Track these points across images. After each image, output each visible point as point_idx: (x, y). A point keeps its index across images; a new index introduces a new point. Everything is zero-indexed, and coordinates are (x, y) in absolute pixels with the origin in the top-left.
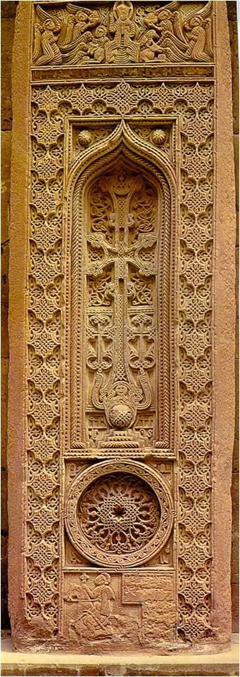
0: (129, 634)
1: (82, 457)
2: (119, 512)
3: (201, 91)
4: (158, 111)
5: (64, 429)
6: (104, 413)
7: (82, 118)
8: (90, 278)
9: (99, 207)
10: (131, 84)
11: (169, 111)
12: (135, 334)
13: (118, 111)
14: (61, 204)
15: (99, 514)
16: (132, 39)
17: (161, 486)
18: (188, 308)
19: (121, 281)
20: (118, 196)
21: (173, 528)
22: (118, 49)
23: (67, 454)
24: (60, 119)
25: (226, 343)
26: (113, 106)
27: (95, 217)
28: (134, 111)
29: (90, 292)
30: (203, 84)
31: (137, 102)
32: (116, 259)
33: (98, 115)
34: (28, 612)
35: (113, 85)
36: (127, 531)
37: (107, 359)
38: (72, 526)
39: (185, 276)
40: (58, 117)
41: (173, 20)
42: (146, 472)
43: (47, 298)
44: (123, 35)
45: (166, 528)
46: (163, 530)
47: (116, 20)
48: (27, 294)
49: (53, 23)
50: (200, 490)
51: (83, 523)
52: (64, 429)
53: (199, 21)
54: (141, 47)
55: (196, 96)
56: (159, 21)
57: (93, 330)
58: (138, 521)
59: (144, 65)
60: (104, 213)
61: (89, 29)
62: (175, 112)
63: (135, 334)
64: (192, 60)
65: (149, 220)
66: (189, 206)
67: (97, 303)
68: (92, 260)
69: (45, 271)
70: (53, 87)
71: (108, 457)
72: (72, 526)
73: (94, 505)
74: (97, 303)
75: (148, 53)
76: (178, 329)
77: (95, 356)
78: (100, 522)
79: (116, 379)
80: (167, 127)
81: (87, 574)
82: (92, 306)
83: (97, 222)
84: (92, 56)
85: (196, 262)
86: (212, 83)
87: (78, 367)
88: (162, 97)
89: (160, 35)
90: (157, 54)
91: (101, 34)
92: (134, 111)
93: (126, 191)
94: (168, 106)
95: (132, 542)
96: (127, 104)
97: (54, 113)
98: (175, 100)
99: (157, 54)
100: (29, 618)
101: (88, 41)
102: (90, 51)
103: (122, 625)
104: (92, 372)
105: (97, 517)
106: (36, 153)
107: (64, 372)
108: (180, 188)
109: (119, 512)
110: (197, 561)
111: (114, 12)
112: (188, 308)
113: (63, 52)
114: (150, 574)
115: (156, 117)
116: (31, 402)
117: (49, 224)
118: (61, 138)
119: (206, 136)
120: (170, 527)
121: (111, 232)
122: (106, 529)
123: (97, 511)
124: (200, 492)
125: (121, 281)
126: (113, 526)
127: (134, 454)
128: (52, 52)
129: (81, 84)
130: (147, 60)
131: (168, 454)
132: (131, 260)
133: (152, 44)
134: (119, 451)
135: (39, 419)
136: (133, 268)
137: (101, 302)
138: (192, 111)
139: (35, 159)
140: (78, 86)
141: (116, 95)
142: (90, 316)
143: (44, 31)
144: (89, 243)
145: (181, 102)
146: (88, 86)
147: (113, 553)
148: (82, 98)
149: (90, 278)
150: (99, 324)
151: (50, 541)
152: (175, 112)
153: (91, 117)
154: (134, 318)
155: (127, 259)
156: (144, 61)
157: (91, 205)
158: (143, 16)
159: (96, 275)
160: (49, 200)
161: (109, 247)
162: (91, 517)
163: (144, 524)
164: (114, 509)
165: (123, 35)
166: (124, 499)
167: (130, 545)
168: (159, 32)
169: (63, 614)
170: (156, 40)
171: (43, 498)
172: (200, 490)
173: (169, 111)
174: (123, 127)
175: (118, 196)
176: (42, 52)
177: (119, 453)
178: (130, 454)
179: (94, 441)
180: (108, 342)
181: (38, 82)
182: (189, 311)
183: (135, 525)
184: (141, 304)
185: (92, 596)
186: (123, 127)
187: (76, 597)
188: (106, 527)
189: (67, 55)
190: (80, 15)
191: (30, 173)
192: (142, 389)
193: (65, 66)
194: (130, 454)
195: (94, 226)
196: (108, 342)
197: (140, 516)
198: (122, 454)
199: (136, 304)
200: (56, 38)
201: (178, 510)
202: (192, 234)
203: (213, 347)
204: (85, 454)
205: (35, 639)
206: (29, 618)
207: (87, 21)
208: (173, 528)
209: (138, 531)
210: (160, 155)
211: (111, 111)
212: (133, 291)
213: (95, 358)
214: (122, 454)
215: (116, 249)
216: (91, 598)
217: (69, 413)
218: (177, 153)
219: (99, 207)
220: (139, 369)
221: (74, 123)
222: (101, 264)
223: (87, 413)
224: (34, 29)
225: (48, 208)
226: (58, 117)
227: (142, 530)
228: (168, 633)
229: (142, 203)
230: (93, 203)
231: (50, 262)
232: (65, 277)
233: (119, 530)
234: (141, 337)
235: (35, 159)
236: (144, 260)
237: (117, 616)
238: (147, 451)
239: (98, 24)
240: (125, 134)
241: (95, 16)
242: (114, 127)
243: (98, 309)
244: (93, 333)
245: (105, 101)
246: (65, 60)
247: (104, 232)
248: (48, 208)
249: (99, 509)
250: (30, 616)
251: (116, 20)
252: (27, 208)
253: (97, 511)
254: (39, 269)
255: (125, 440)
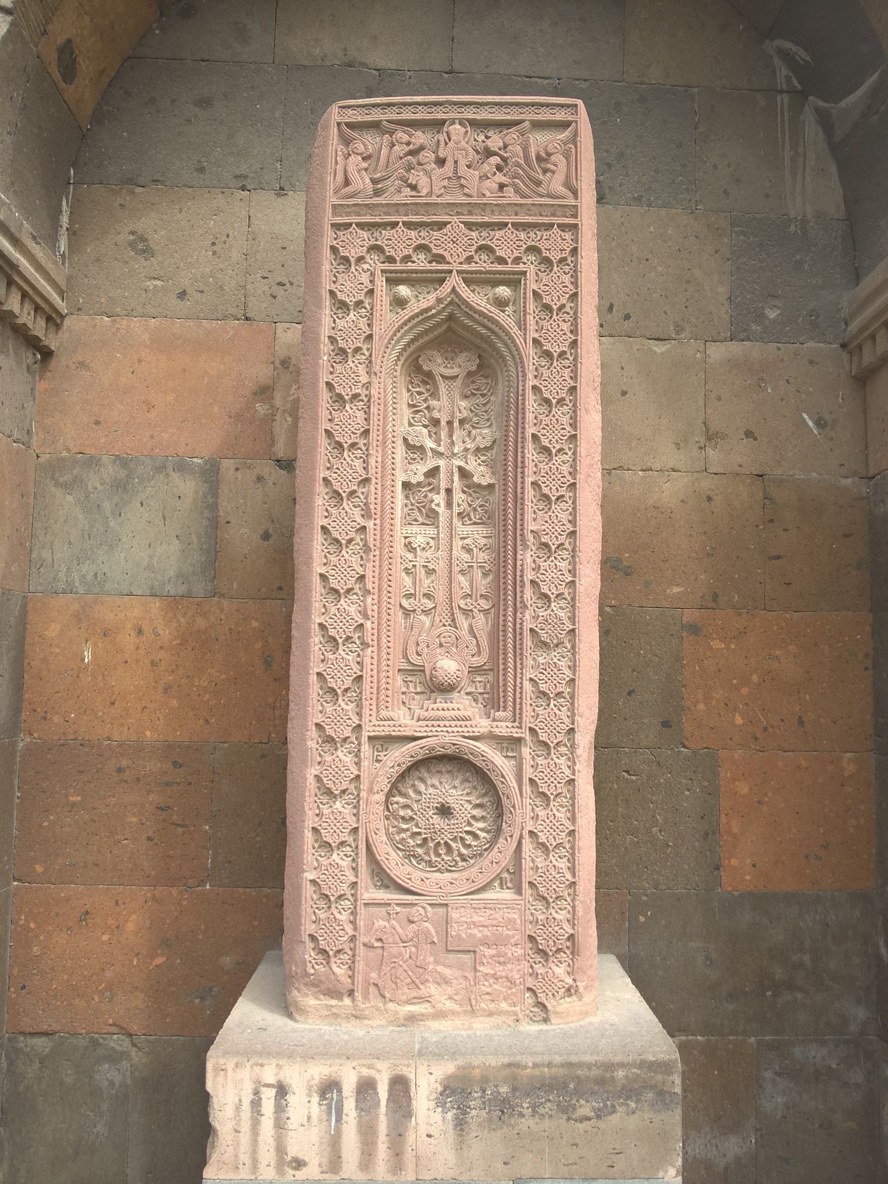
0: (456, 994)
1: (393, 734)
2: (445, 811)
3: (561, 236)
4: (502, 261)
5: (368, 693)
6: (423, 671)
7: (399, 266)
8: (406, 485)
9: (419, 393)
10: (469, 226)
11: (517, 260)
12: (467, 562)
13: (449, 258)
14: (369, 383)
15: (416, 814)
16: (469, 167)
17: (503, 776)
18: (543, 527)
19: (449, 491)
20: (444, 377)
21: (521, 837)
22: (449, 178)
23: (371, 729)
24: (368, 270)
25: (590, 579)
26: (441, 252)
27: (414, 406)
28: (469, 259)
29: (406, 506)
30: (563, 227)
31: (474, 247)
32: (441, 463)
33: (421, 262)
34: (310, 962)
35: (441, 225)
36: (454, 839)
37: (427, 596)
38: (376, 834)
39: (540, 482)
40: (366, 266)
41: (526, 150)
42: (483, 756)
43: (349, 510)
44: (456, 162)
45: (511, 836)
46: (506, 840)
47: (446, 144)
48: (321, 503)
49: (362, 146)
50: (559, 783)
51: (393, 827)
52: (368, 693)
53: (558, 147)
54: (480, 178)
55: (554, 244)
56: (505, 146)
57: (410, 556)
58: (469, 824)
59: (485, 201)
60: (425, 400)
61: (412, 153)
62: (525, 263)
63: (467, 562)
64: (549, 196)
65: (486, 411)
66: (543, 389)
67: (416, 520)
68: (409, 463)
69: (345, 472)
70: (361, 225)
71: (430, 734)
72: (376, 834)
73: (409, 802)
74: (416, 520)
75: (491, 185)
76: (529, 555)
77: (413, 592)
78: (417, 826)
79: (441, 624)
80: (514, 281)
81: (397, 904)
82: (409, 524)
83: (417, 412)
84: (414, 187)
85: (554, 464)
86: (575, 226)
87: (389, 606)
88: (507, 244)
89: (507, 165)
90: (502, 186)
91: (427, 160)
92: (469, 259)
93: (455, 371)
94: (516, 254)
95: (460, 855)
96: (460, 250)
97: (360, 259)
98: (525, 246)
99: (502, 186)
100: (312, 971)
101: (409, 168)
102: (412, 180)
103: (446, 983)
104: (407, 613)
105: (412, 819)
106: (335, 314)
107: (369, 613)
108: (531, 364)
109: (445, 811)
110: (554, 886)
111: (445, 134)
112: (543, 527)
113: (374, 181)
114: (489, 906)
115: (500, 268)
116: (323, 654)
117: (351, 409)
118: (371, 292)
119: (568, 296)
120: (516, 836)
121: (435, 426)
122: (424, 836)
123: (413, 810)
124: (558, 785)
125: (449, 491)
126: (435, 832)
127: (466, 729)
128: (362, 182)
129: (398, 223)
130: (488, 194)
131: (514, 730)
132: (462, 464)
133: (495, 173)
134: (445, 726)
135: (333, 678)
136: (464, 474)
137: (420, 519)
138: (547, 261)
139: (334, 321)
140: (394, 225)
141: (446, 237)
142: (406, 538)
143: (350, 155)
144: (405, 440)
145: (533, 249)
146: (408, 225)
147: (435, 871)
148: (399, 242)
149: (406, 485)
150: (418, 549)
151: (345, 855)
152: (525, 263)
153: (410, 266)
154: (466, 541)
155: (458, 462)
156: (484, 195)
157: (409, 390)
158: (483, 142)
159: (414, 482)
160: (353, 375)
161: (434, 446)
162: (403, 818)
163: (478, 829)
164: (436, 807)
165: (456, 162)
166: (455, 792)
167: (458, 859)
168: (504, 160)
169: (360, 966)
170: (499, 168)
171: (336, 792)
172: (559, 783)
173: (517, 260)
174: (454, 280)
175: (444, 377)
176: (347, 183)
177: (444, 729)
178: (460, 729)
179: (409, 709)
180: (430, 572)
181: (339, 220)
182: (544, 530)
183: (466, 832)
184: (475, 523)
185: (404, 938)
186: (454, 280)
187: (381, 940)
188: (425, 834)
189: (380, 186)
190: (399, 135)
191: (326, 339)
192: (476, 639)
193: (376, 200)
194: (460, 729)
195: (413, 418)
196: (430, 572)
197: (474, 817)
198: (450, 729)
199: (469, 522)
200: (365, 165)
201: (523, 811)
202: (547, 425)
203: (577, 581)
204: (396, 729)
205: (320, 1002)
206: (312, 971)
207: (408, 143)
208: (521, 837)
209: (469, 839)
210: (506, 318)
211: (439, 259)
212: (465, 505)
213: (412, 594)
214: (450, 729)
215: (441, 449)
216: (403, 942)
217: (375, 671)
218: (528, 316)
219: (419, 393)
220: (471, 611)
221: (388, 275)
222: (422, 468)
223: (399, 670)
224: (336, 153)
225: (350, 387)
226: (366, 266)
227: (475, 836)
228: (512, 994)
229: (475, 390)
230: (410, 387)
231: (352, 460)
232: (374, 481)
233: (443, 839)
234: (475, 567)
235: (334, 321)
236: (479, 464)
237: (440, 968)
238: (483, 725)
239: (422, 148)
240: (458, 289)
241: (420, 137)
242: (442, 281)
243: (415, 529)
244: (410, 561)
245: (432, 245)
246: (377, 193)
247: (425, 426)
248: (350, 387)
249: (415, 806)
250: (313, 967)
251: (446, 144)
252: (322, 386)
253: (413, 810)
254: (338, 468)
255: (453, 709)
